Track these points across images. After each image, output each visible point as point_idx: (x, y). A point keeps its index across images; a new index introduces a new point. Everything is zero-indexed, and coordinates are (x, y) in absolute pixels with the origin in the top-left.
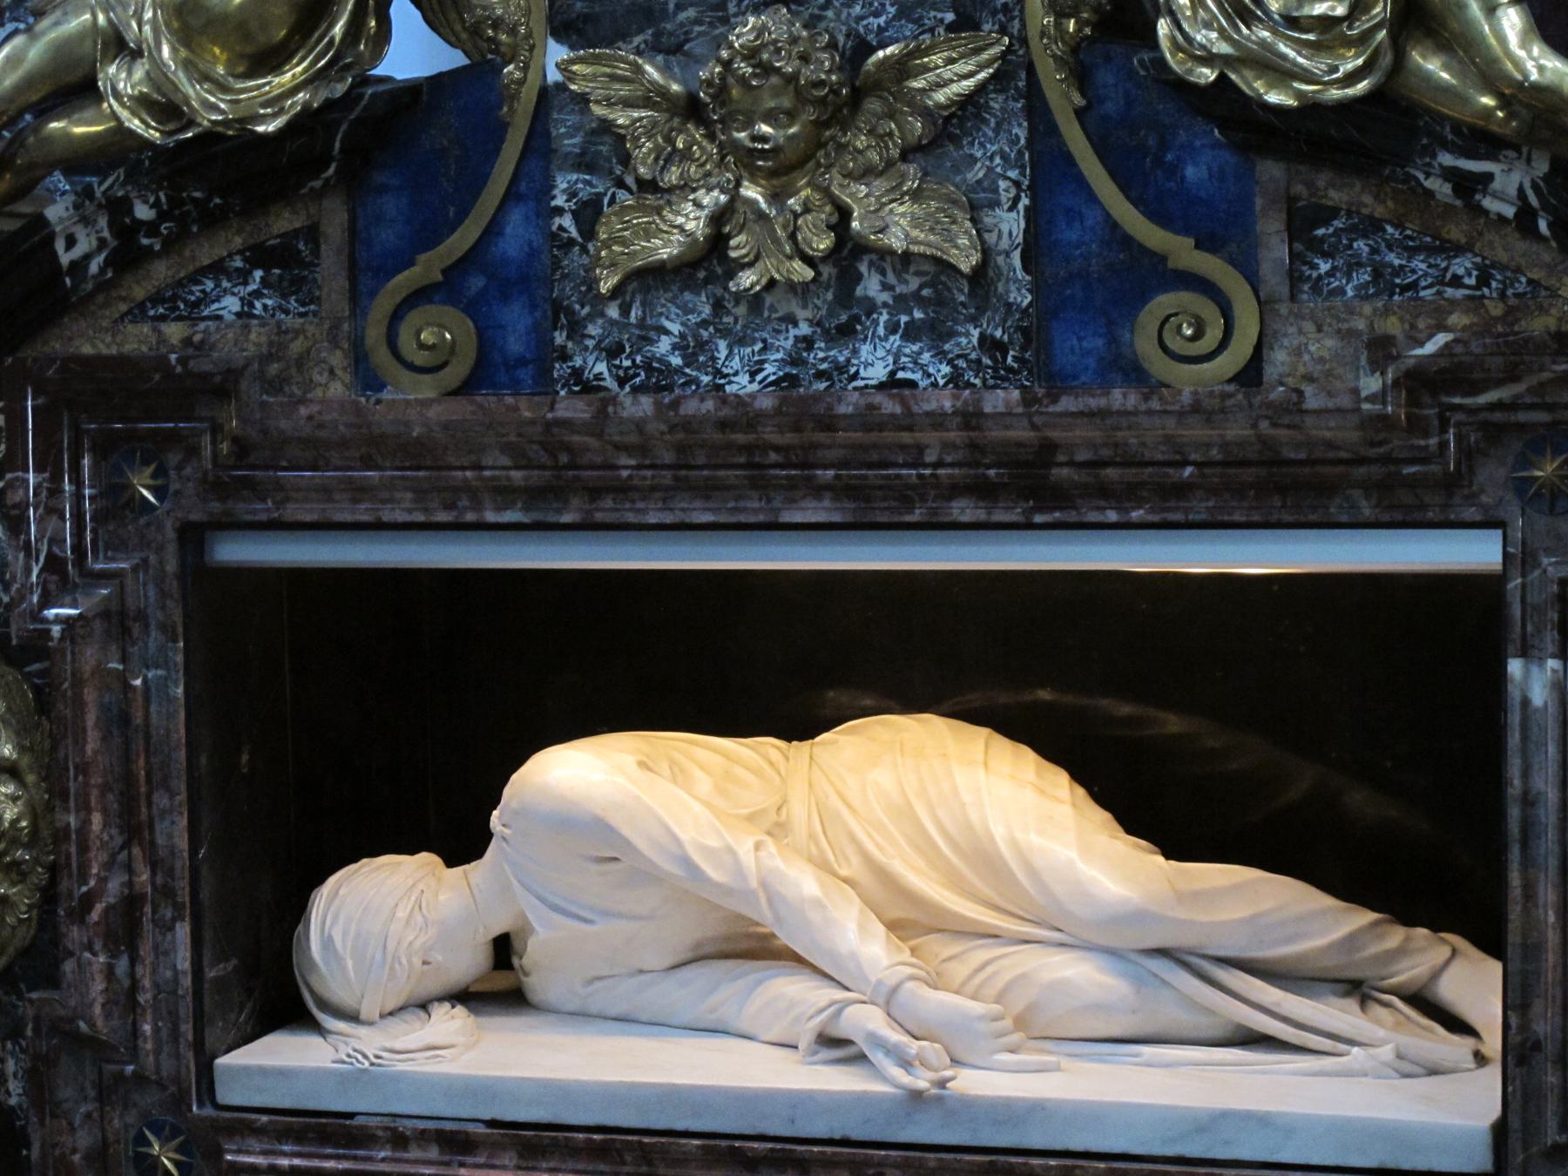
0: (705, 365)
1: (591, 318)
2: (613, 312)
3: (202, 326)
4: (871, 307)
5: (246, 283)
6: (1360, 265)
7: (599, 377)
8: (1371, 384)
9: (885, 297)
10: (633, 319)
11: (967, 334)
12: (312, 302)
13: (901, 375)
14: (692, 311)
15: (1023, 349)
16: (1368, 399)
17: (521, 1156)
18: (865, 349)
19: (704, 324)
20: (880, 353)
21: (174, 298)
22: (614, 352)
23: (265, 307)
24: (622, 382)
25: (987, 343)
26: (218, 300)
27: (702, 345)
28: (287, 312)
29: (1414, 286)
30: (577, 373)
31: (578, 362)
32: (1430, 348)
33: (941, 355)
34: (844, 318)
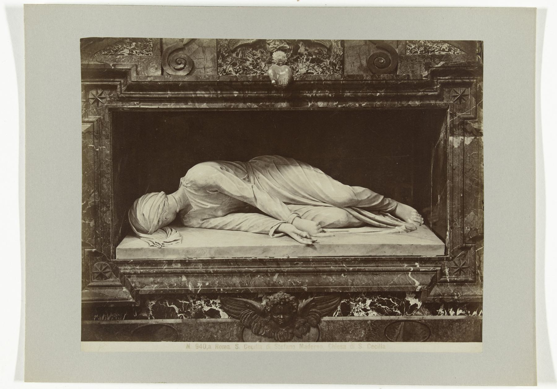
0: (258, 68)
1: (228, 56)
2: (234, 55)
3: (118, 57)
4: (301, 55)
5: (131, 46)
6: (421, 46)
7: (230, 71)
8: (426, 73)
9: (306, 52)
10: (239, 57)
11: (327, 62)
12: (150, 51)
13: (309, 71)
14: (255, 55)
15: (341, 65)
16: (424, 77)
17: (203, 265)
18: (300, 65)
19: (259, 58)
20: (304, 66)
21: (110, 49)
22: (234, 65)
23: (136, 52)
24: (236, 73)
25: (332, 64)
26: (122, 50)
27: (257, 64)
28: (143, 54)
29: (434, 51)
30: (224, 70)
31: (225, 67)
32: (439, 65)
33: (319, 66)
34: (295, 57)
